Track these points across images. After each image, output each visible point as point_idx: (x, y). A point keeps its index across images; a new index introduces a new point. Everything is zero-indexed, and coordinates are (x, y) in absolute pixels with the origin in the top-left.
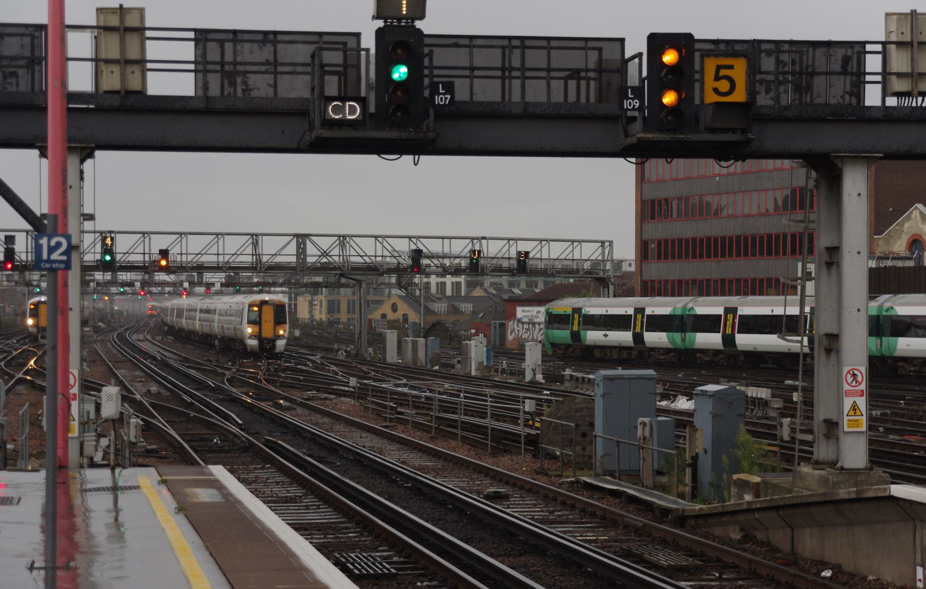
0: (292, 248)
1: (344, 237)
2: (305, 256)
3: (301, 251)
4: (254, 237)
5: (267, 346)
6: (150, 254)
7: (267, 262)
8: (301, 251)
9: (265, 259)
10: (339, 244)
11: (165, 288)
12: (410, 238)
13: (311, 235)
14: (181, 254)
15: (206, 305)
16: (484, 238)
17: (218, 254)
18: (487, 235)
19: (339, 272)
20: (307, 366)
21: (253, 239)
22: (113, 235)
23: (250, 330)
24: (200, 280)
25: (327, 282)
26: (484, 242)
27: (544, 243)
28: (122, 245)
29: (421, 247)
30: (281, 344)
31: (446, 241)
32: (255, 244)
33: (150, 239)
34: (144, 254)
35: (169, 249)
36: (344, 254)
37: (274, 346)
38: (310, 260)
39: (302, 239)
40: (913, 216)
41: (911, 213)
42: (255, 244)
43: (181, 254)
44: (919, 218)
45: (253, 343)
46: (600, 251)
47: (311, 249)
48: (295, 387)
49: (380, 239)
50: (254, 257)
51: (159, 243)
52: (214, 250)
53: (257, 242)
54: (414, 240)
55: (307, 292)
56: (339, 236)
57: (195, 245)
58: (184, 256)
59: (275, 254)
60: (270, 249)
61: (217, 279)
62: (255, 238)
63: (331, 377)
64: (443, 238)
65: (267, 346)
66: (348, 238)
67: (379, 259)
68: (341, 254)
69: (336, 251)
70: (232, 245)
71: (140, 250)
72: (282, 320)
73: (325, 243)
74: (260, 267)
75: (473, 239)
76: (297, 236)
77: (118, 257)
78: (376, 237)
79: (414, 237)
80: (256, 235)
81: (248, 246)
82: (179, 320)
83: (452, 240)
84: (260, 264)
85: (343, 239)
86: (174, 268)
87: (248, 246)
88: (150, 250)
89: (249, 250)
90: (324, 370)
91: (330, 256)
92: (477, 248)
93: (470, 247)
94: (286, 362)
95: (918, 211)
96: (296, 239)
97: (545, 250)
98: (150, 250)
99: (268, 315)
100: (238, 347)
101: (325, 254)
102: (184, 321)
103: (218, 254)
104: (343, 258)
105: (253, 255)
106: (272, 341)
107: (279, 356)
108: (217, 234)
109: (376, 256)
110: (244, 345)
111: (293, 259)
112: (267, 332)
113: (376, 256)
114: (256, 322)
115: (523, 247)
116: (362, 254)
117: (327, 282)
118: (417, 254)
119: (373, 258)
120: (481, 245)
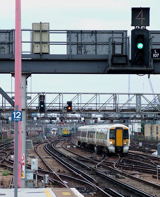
0: (134, 101)
3: (139, 102)
4: (115, 95)
5: (119, 150)
7: (122, 107)
8: (139, 102)
11: (74, 120)
15: (100, 130)
17: (96, 104)
19: (158, 113)
20: (139, 160)
21: (114, 96)
22: (44, 94)
23: (111, 143)
24: (90, 116)
25: (156, 118)
28: (48, 100)
30: (126, 149)
32: (115, 99)
34: (60, 104)
37: (122, 150)
42: (115, 99)
45: (112, 149)
47: (143, 101)
48: (129, 170)
50: (115, 105)
51: (66, 99)
52: (94, 102)
55: (149, 122)
57: (85, 99)
60: (122, 101)
61: (99, 116)
62: (115, 96)
63: (149, 165)
65: (119, 150)
70: (103, 99)
72: (126, 137)
74: (118, 110)
76: (137, 94)
77: (47, 105)
80: (116, 94)
81: (112, 99)
82: (83, 138)
86: (74, 111)
87: (112, 99)
89: (112, 102)
90: (147, 162)
94: (130, 158)
99: (119, 134)
100: (105, 150)
102: (87, 138)
105: (114, 104)
106: (122, 148)
107: (127, 154)
110: (108, 150)
111: (135, 105)
112: (119, 144)
114: (113, 138)
117: (156, 118)
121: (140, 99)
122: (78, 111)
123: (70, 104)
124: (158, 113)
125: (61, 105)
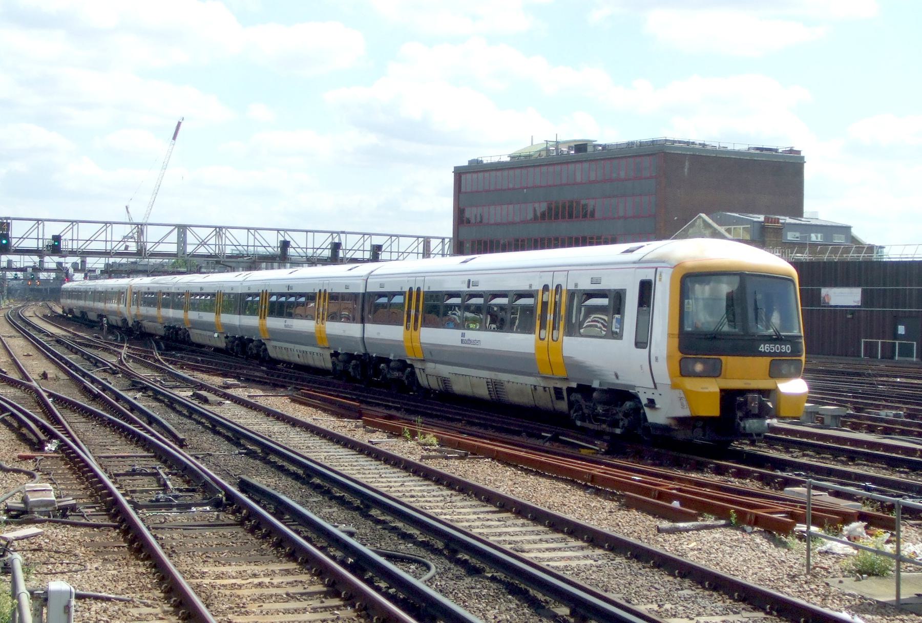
0: (174, 237)
1: (221, 228)
2: (185, 243)
4: (140, 226)
6: (43, 239)
9: (149, 246)
10: (215, 235)
12: (278, 230)
13: (190, 226)
14: (73, 240)
16: (343, 232)
17: (106, 241)
18: (347, 230)
21: (138, 228)
22: (9, 221)
26: (343, 236)
27: (393, 238)
29: (288, 239)
31: (310, 234)
32: (141, 233)
33: (44, 225)
34: (38, 239)
35: (61, 235)
36: (220, 243)
38: (190, 249)
39: (182, 229)
40: (697, 224)
41: (695, 221)
43: (73, 240)
44: (702, 225)
46: (440, 247)
47: (190, 238)
49: (252, 231)
51: (52, 230)
52: (103, 237)
53: (142, 231)
54: (282, 233)
56: (216, 227)
57: (85, 231)
58: (75, 242)
59: (158, 242)
62: (140, 228)
64: (307, 231)
66: (224, 229)
67: (251, 249)
68: (217, 243)
69: (212, 241)
71: (34, 235)
73: (204, 233)
74: (145, 253)
75: (332, 233)
77: (14, 241)
78: (248, 229)
79: (283, 230)
80: (141, 225)
83: (315, 233)
84: (145, 251)
85: (219, 230)
88: (43, 235)
91: (208, 245)
92: (336, 240)
93: (330, 240)
95: (701, 219)
96: (177, 229)
97: (395, 245)
98: (43, 235)
101: (203, 243)
103: (106, 241)
104: (219, 247)
108: (106, 223)
109: (248, 246)
113: (248, 246)
115: (377, 241)
116: (236, 243)
118: (285, 245)
119: (246, 248)
120: (340, 239)
121: (185, 234)
122: (73, 253)
123: (57, 238)
124: (215, 259)
125: (40, 241)
